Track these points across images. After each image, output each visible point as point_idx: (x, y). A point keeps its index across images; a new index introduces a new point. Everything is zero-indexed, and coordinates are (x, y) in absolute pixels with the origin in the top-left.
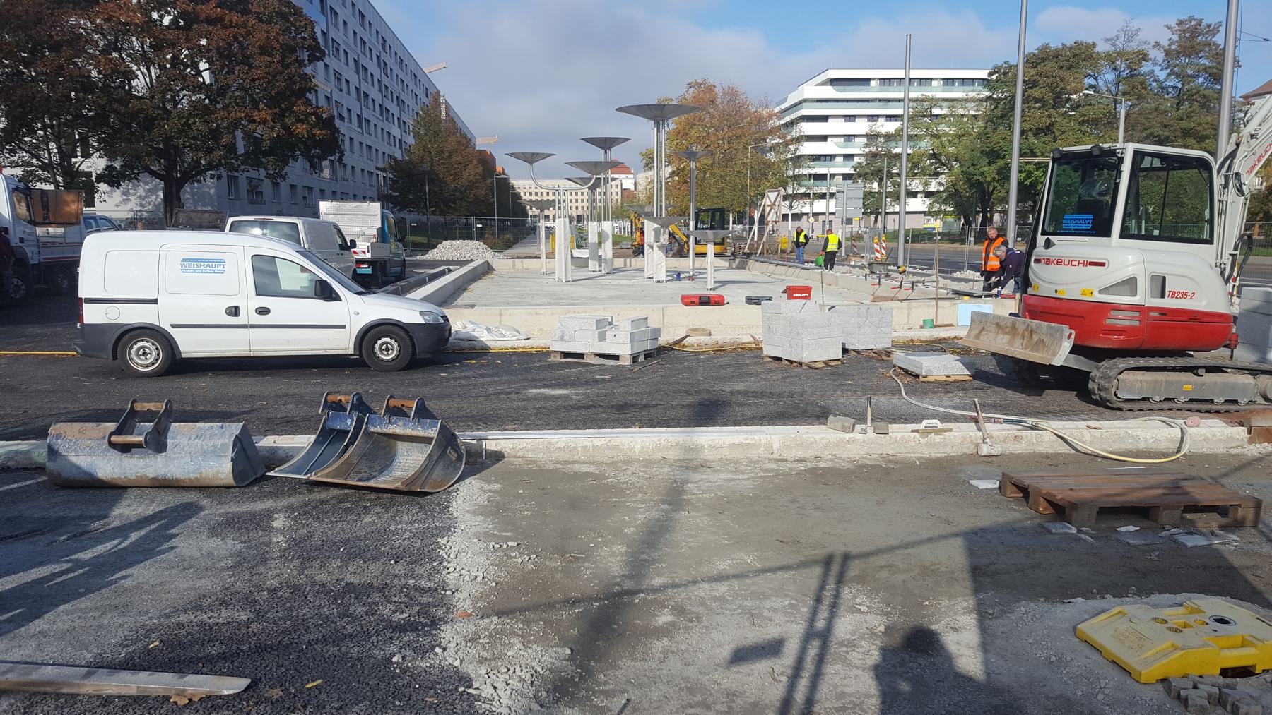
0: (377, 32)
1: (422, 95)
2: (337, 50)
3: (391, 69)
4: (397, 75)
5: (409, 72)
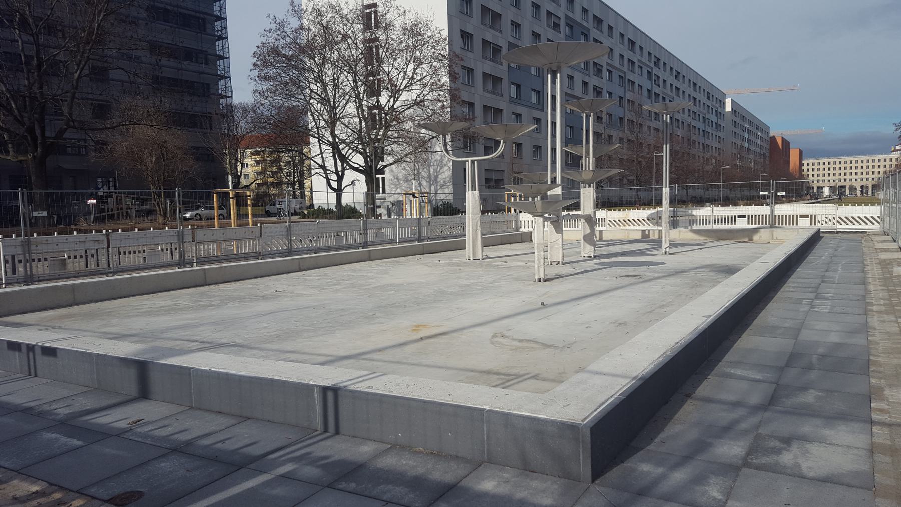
0: (650, 54)
1: (702, 97)
2: (600, 71)
3: (665, 81)
4: (671, 85)
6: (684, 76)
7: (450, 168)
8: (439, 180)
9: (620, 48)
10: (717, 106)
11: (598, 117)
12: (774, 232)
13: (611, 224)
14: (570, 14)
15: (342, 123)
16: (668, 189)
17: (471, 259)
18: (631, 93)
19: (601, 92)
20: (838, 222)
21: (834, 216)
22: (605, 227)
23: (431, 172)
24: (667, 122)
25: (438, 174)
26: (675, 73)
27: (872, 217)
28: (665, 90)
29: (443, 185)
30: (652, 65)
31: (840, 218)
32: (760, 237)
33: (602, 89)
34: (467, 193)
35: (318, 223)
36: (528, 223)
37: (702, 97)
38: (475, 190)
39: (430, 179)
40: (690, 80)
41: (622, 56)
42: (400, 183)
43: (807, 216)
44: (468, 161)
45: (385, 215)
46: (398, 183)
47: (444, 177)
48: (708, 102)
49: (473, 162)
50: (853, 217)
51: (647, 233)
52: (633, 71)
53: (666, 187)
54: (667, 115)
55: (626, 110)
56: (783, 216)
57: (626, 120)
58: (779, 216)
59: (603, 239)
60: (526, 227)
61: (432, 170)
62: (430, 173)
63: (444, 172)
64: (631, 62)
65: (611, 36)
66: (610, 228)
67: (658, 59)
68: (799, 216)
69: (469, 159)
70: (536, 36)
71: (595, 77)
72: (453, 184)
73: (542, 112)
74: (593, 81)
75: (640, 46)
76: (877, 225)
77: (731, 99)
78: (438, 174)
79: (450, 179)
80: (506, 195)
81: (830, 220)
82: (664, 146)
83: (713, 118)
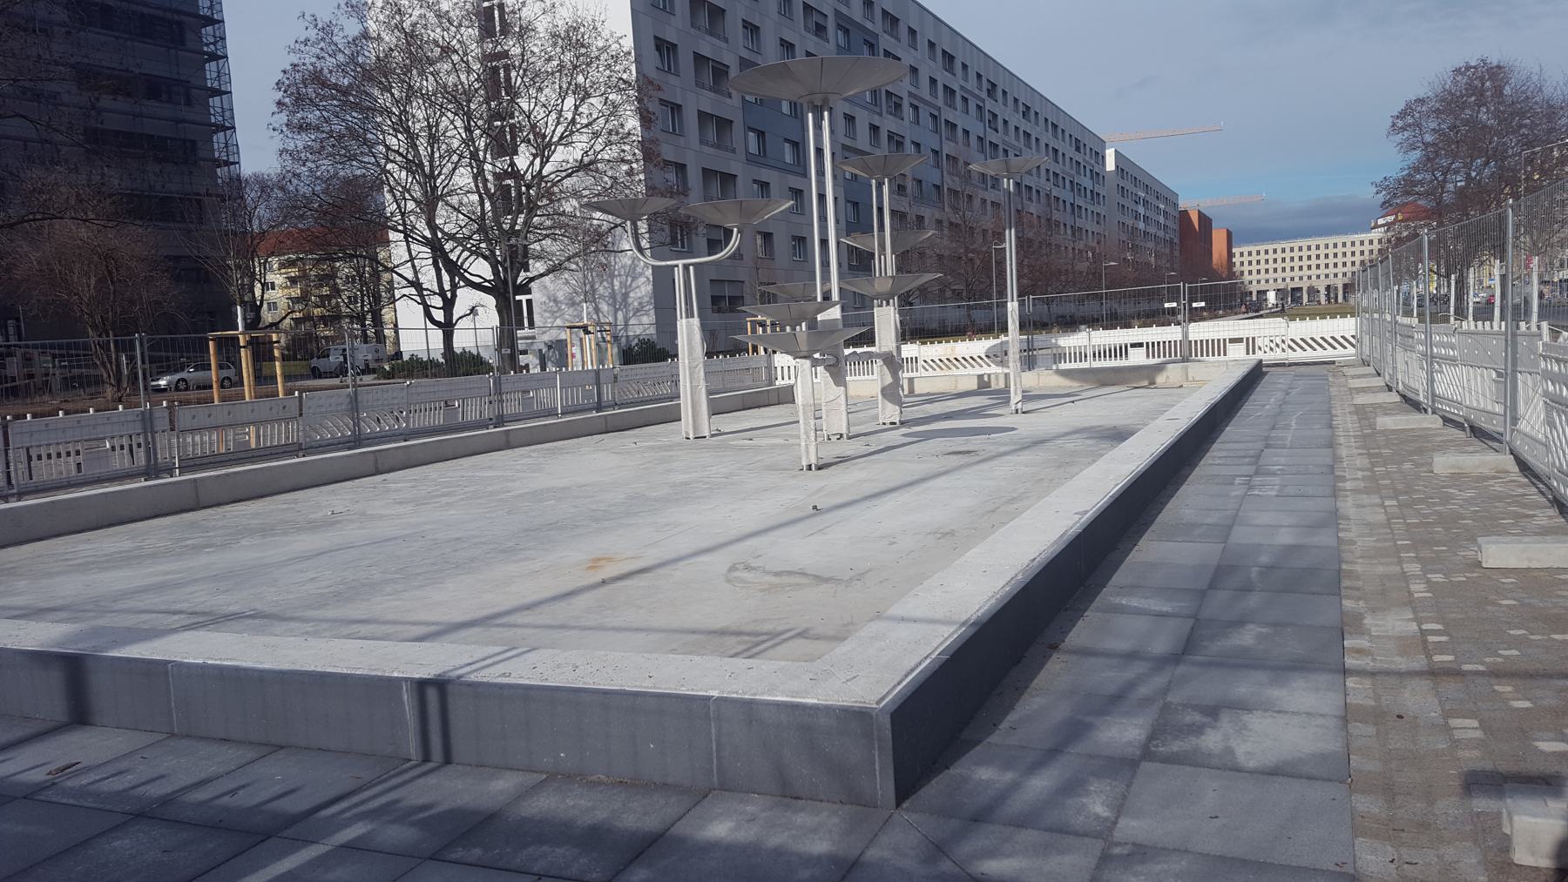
0: (979, 76)
1: (1067, 149)
2: (898, 106)
3: (1005, 122)
4: (1017, 128)
5: (1042, 121)
6: (1036, 113)
7: (648, 279)
8: (630, 300)
9: (931, 68)
10: (1093, 162)
11: (898, 185)
12: (1189, 369)
13: (927, 367)
14: (844, 10)
15: (447, 204)
16: (1016, 304)
17: (691, 436)
18: (952, 144)
19: (902, 143)
20: (1290, 347)
21: (1284, 338)
22: (917, 371)
23: (616, 288)
24: (1010, 192)
25: (628, 290)
26: (1021, 108)
27: (1342, 337)
28: (1007, 139)
29: (638, 310)
30: (984, 95)
31: (1292, 340)
32: (1168, 377)
33: (903, 137)
34: (678, 322)
35: (408, 385)
36: (789, 371)
37: (1067, 149)
38: (693, 316)
39: (615, 300)
40: (1046, 120)
41: (933, 81)
42: (559, 309)
43: (1240, 340)
44: (677, 266)
45: (535, 367)
46: (556, 309)
47: (639, 295)
48: (1078, 157)
49: (686, 267)
50: (1312, 339)
51: (986, 379)
52: (952, 106)
53: (1013, 301)
54: (1009, 180)
55: (945, 173)
56: (1201, 341)
57: (946, 190)
58: (1196, 342)
59: (916, 393)
60: (786, 377)
61: (616, 283)
62: (613, 290)
63: (638, 287)
64: (949, 91)
65: (913, 45)
66: (926, 374)
67: (994, 85)
68: (1129, 346)
69: (680, 263)
70: (787, 46)
71: (891, 117)
72: (655, 308)
73: (805, 179)
74: (888, 124)
75: (963, 64)
76: (1351, 350)
77: (1113, 149)
78: (628, 290)
79: (651, 298)
80: (749, 323)
81: (1277, 345)
82: (1007, 232)
83: (1086, 182)
